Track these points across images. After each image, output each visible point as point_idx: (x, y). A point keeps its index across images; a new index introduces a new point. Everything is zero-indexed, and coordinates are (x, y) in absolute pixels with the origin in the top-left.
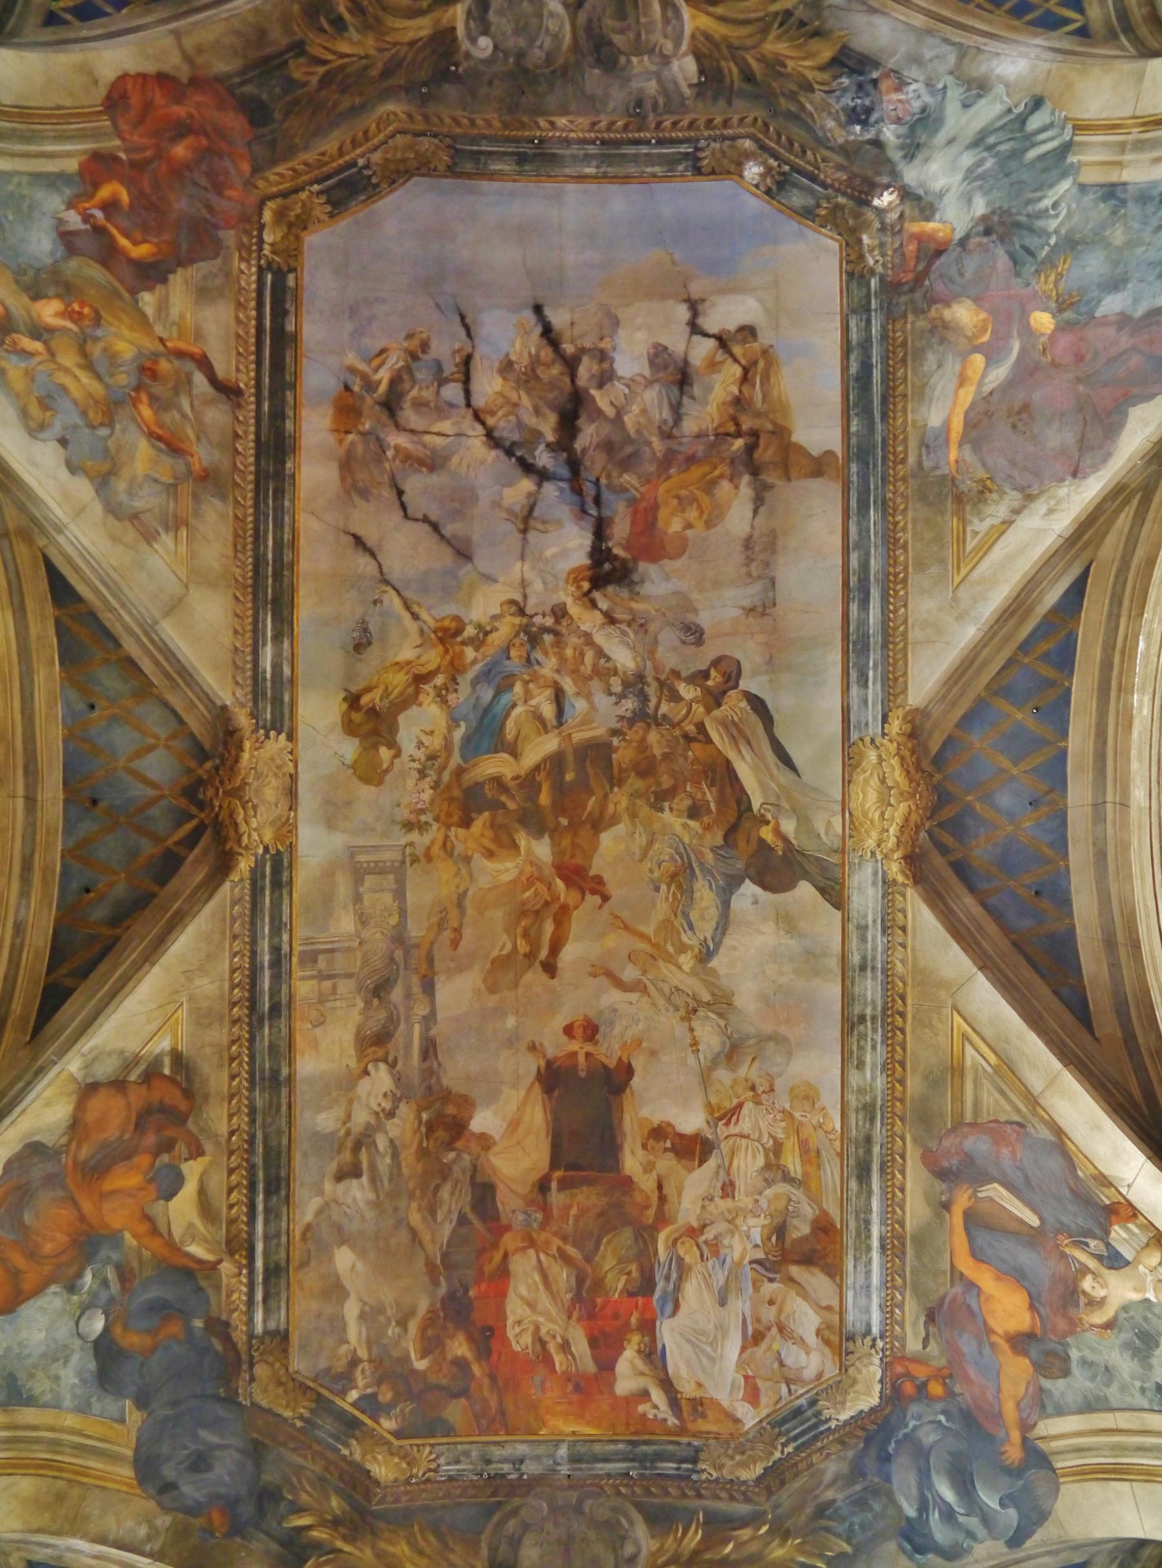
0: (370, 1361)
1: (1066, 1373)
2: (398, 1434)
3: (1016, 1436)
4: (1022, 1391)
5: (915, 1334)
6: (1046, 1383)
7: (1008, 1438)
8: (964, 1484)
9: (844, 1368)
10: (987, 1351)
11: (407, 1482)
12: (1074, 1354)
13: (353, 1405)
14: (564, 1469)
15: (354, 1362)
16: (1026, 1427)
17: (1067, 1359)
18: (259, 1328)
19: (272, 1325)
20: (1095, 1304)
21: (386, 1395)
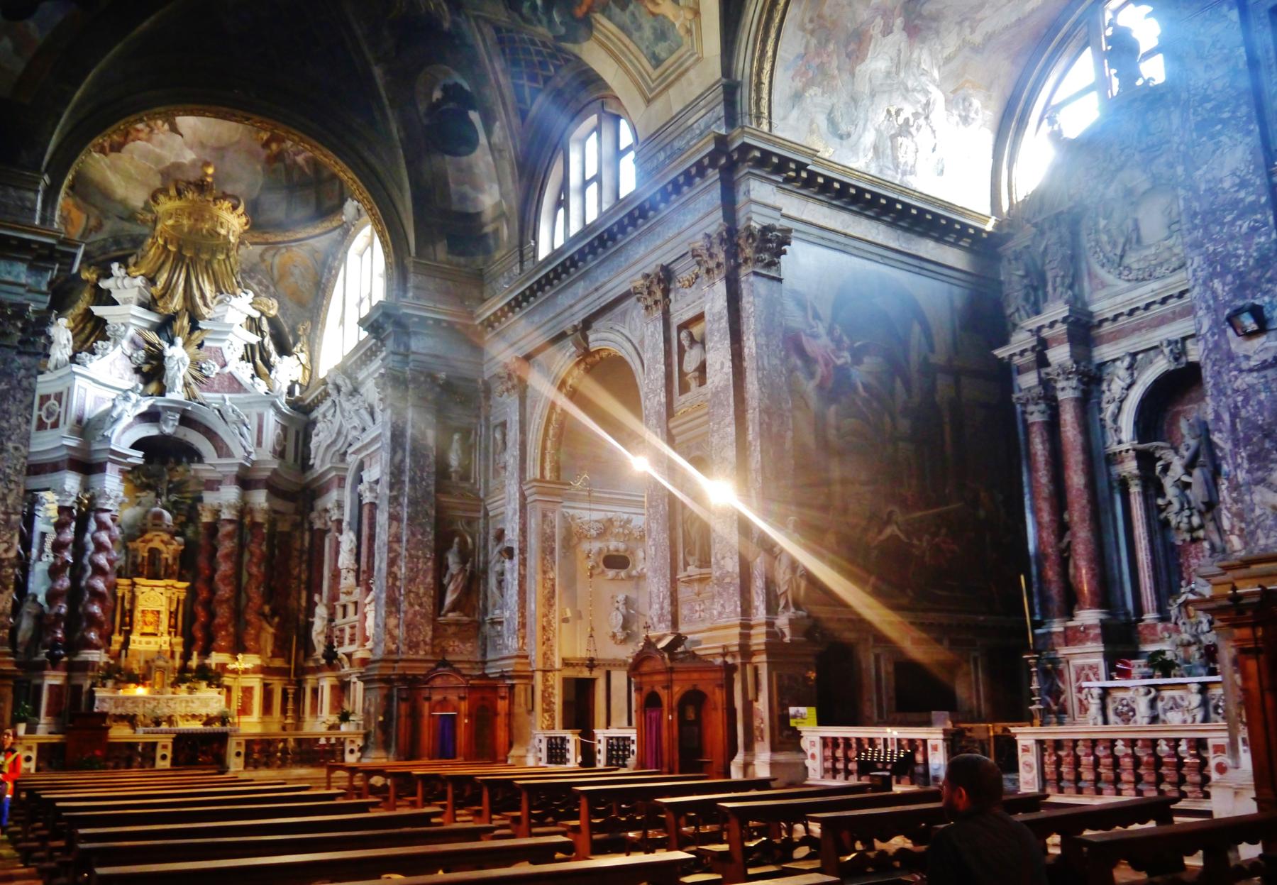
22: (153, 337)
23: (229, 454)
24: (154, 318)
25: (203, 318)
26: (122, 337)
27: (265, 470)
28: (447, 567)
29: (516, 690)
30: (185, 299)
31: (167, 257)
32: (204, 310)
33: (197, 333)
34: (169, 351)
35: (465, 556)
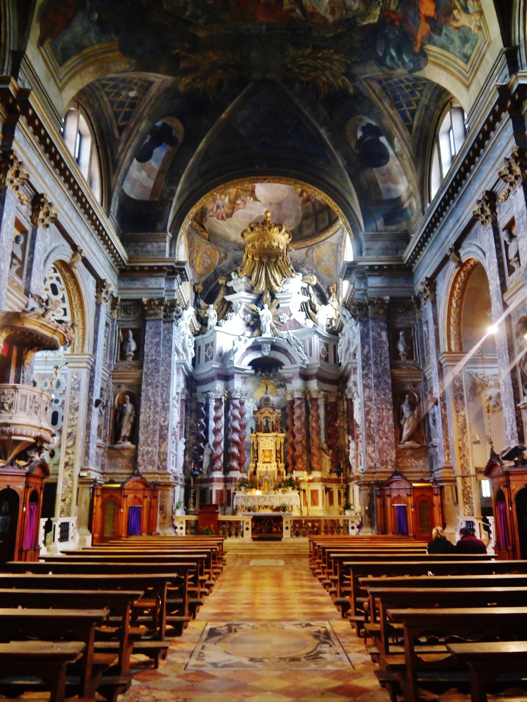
1: (440, 34)
3: (419, 45)
4: (425, 33)
5: (394, 4)
6: (433, 35)
7: (416, 45)
8: (399, 53)
9: (367, 9)
10: (417, 18)
12: (444, 31)
16: (423, 44)
17: (441, 31)
20: (455, 20)
22: (254, 307)
23: (295, 363)
24: (253, 297)
25: (277, 292)
26: (239, 309)
27: (315, 368)
28: (403, 414)
29: (445, 490)
30: (266, 284)
31: (255, 264)
32: (277, 288)
33: (275, 301)
34: (261, 313)
35: (413, 405)
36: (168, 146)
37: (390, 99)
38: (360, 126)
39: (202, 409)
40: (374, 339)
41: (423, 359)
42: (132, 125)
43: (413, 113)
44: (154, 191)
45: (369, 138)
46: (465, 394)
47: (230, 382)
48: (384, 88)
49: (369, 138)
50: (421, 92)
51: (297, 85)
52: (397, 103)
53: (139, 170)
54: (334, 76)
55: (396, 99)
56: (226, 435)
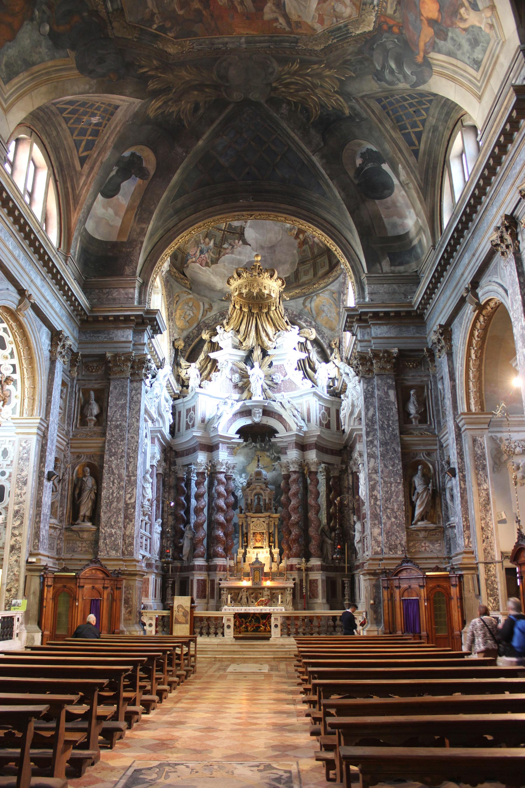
0: (159, 13)
2: (175, 38)
11: (182, 53)
13: (155, 30)
14: (244, 46)
15: (153, 14)
18: (110, 9)
19: (115, 7)
21: (168, 25)
32: (267, 343)
36: (138, 179)
37: (392, 120)
38: (359, 153)
39: (183, 485)
40: (380, 399)
41: (439, 422)
42: (95, 155)
43: (419, 135)
44: (122, 231)
45: (370, 165)
46: (488, 463)
47: (214, 453)
48: (384, 107)
49: (370, 165)
50: (427, 110)
51: (284, 106)
52: (400, 124)
53: (105, 207)
54: (327, 95)
55: (399, 119)
56: (210, 515)
